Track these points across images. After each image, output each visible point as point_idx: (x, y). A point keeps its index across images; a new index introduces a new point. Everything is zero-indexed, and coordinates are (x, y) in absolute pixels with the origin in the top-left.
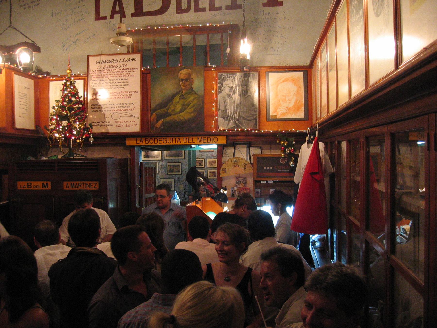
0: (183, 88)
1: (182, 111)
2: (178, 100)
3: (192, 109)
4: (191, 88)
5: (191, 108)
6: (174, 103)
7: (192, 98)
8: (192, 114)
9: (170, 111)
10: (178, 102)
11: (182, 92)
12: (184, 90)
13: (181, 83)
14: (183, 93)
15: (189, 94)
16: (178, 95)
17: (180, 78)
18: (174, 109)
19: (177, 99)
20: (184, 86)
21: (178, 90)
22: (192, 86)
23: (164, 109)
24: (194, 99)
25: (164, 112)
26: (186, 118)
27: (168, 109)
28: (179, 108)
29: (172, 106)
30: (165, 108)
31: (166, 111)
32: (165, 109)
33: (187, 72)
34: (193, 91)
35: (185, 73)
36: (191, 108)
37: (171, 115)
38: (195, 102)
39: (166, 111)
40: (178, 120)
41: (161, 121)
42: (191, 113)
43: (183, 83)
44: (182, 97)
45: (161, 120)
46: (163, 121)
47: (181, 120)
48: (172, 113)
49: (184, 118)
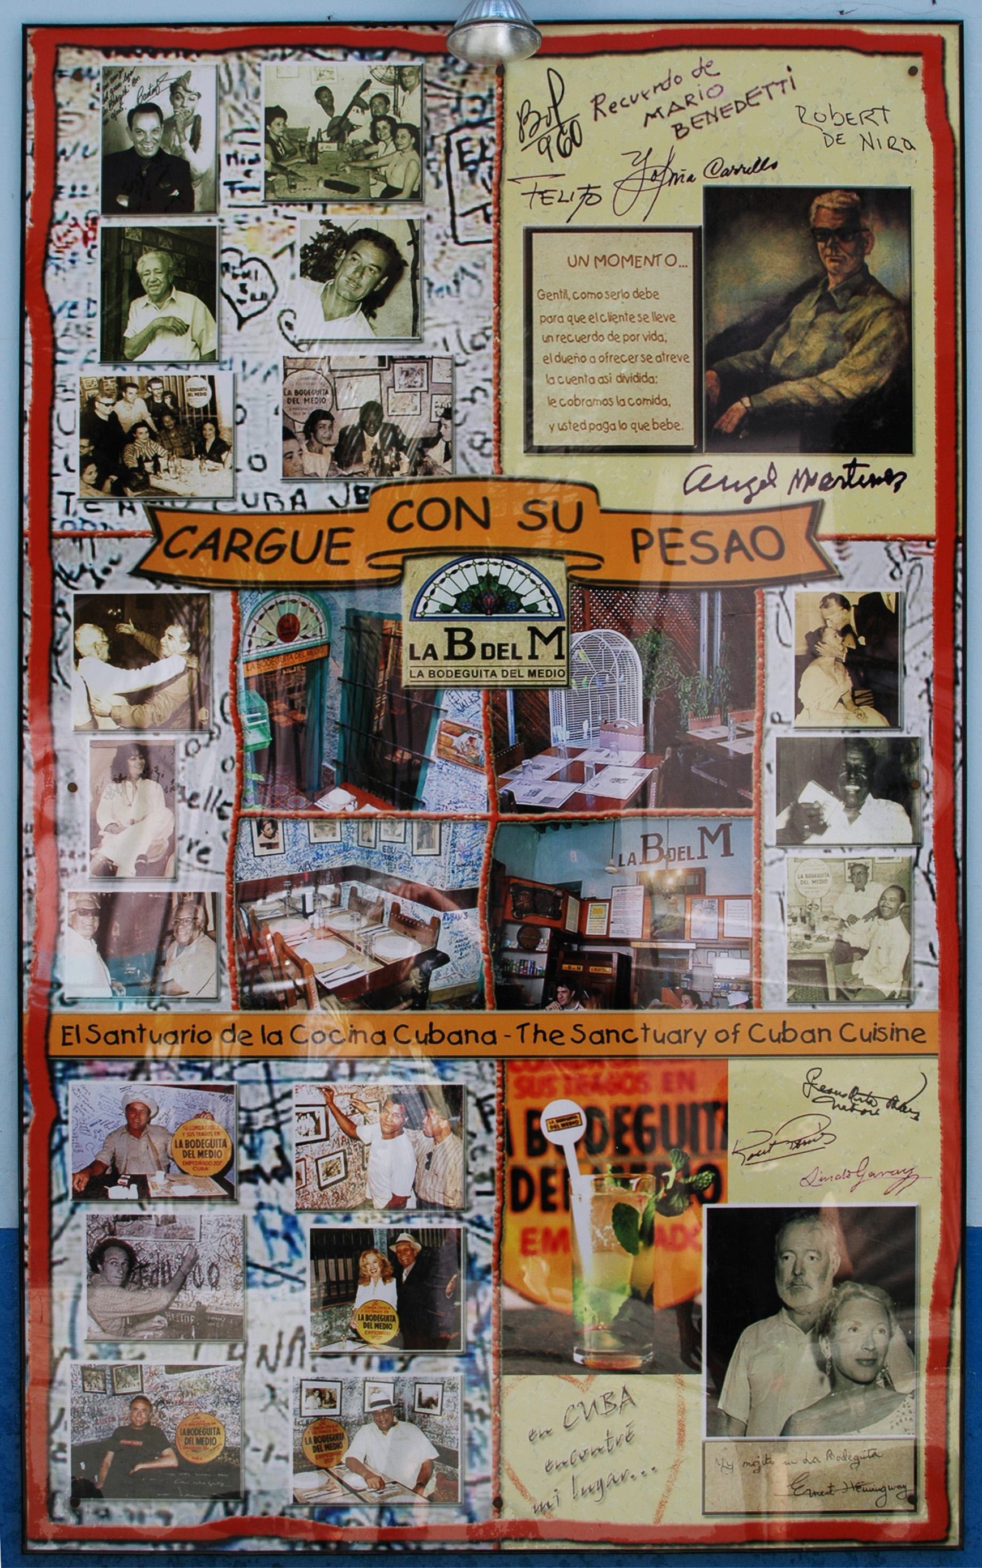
0: (830, 266)
1: (824, 365)
2: (811, 314)
3: (872, 355)
4: (864, 268)
5: (868, 348)
6: (793, 327)
7: (868, 310)
8: (872, 378)
9: (777, 360)
10: (812, 325)
11: (827, 283)
12: (834, 275)
13: (821, 245)
14: (832, 286)
15: (853, 294)
16: (808, 297)
17: (820, 225)
18: (794, 357)
19: (804, 312)
20: (832, 261)
21: (810, 274)
22: (867, 260)
23: (750, 354)
24: (876, 314)
25: (751, 366)
26: (843, 392)
27: (768, 356)
28: (816, 345)
29: (785, 340)
30: (756, 347)
31: (761, 358)
32: (759, 354)
33: (844, 203)
34: (872, 280)
35: (838, 206)
36: (868, 348)
37: (780, 379)
38: (882, 324)
39: (761, 358)
40: (812, 401)
41: (738, 405)
42: (866, 373)
43: (831, 247)
44: (827, 303)
45: (738, 399)
46: (748, 405)
47: (825, 401)
48: (785, 372)
49: (839, 393)
